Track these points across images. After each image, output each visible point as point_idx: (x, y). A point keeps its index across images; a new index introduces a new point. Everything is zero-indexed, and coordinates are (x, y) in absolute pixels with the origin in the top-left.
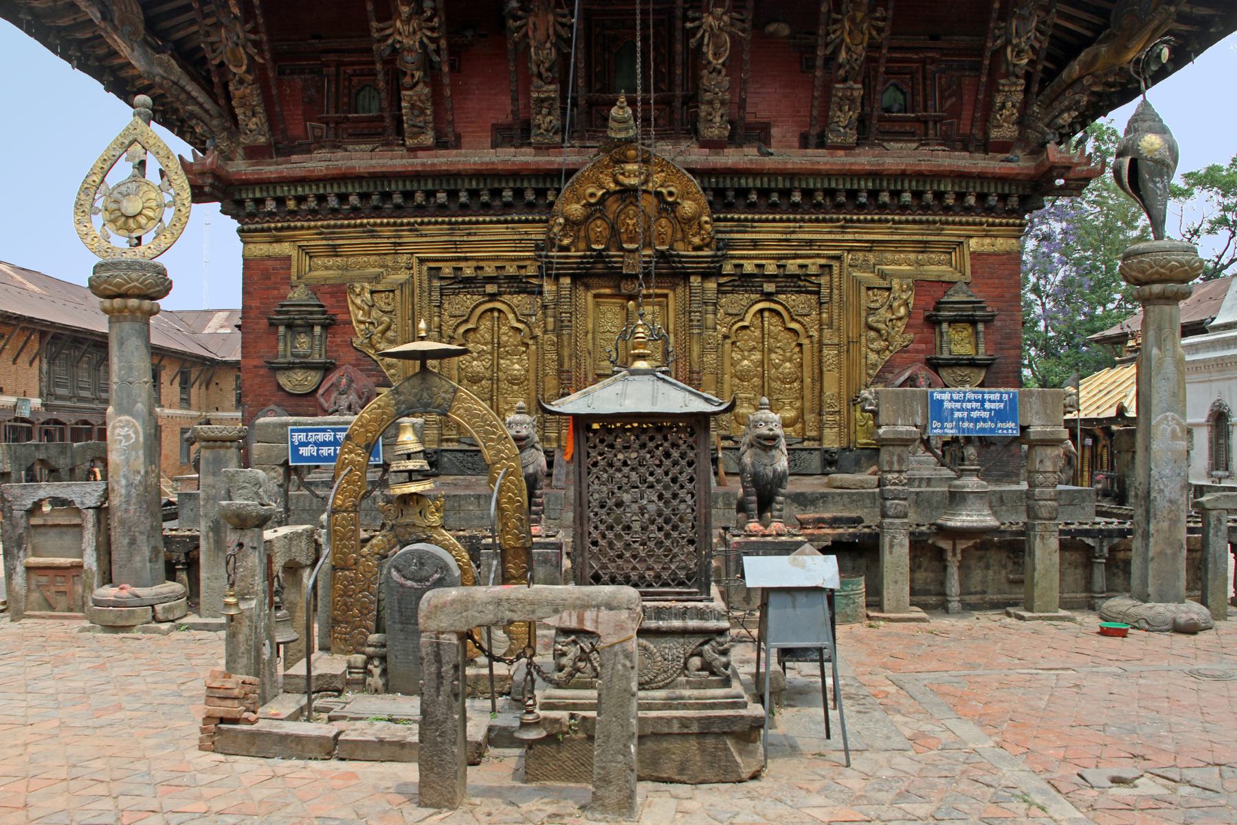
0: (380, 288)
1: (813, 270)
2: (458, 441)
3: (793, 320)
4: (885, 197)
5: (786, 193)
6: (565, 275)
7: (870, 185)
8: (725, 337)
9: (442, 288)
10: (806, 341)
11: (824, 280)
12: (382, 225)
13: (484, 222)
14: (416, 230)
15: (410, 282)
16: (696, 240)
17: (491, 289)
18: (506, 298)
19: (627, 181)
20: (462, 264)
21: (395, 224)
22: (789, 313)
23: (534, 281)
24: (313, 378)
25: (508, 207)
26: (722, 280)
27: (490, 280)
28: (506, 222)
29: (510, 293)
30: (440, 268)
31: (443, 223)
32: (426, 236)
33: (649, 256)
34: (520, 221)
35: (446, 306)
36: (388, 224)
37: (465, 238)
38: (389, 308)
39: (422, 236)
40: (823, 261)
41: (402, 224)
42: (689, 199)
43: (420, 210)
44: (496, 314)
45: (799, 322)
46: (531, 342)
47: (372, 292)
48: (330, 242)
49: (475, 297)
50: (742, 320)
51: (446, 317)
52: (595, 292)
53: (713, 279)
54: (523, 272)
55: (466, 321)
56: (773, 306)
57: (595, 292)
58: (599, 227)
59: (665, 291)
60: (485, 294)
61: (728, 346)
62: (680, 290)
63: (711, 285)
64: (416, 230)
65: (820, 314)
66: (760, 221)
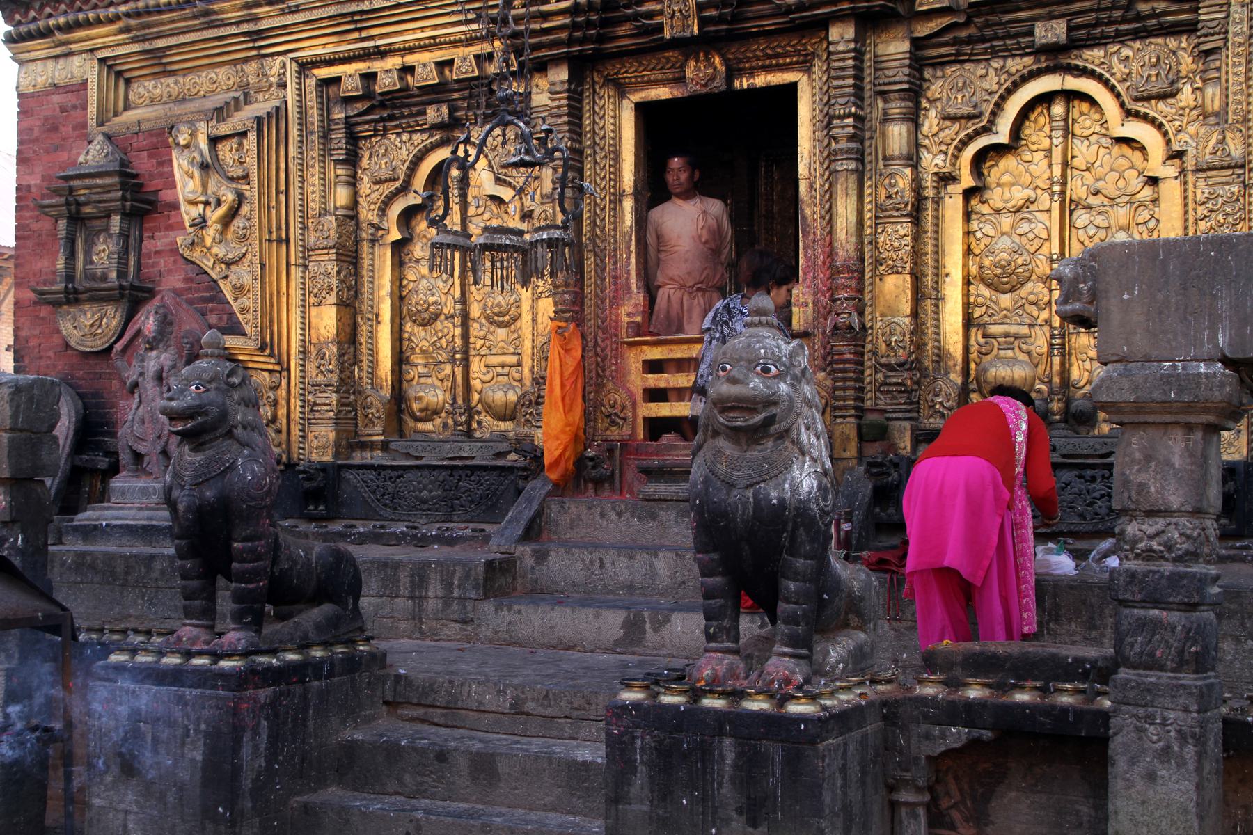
0: (224, 129)
2: (385, 446)
3: (1129, 114)
6: (556, 61)
8: (946, 179)
9: (349, 126)
15: (279, 114)
17: (433, 114)
24: (112, 317)
26: (925, 29)
30: (337, 80)
35: (365, 162)
38: (240, 172)
45: (1145, 118)
48: (147, 46)
49: (417, 138)
50: (986, 130)
51: (365, 187)
53: (901, 31)
55: (405, 188)
56: (1073, 83)
61: (953, 206)
62: (818, 68)
63: (895, 47)
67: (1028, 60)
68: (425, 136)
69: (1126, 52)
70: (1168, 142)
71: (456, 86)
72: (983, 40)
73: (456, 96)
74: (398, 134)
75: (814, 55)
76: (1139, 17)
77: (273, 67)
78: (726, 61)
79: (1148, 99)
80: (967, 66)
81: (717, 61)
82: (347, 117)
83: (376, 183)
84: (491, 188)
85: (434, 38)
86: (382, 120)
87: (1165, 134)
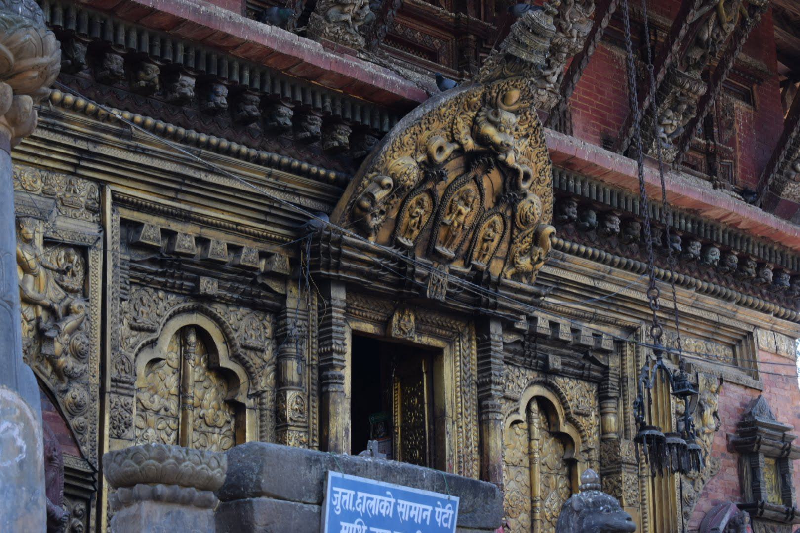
1: (607, 344)
3: (569, 419)
4: (696, 248)
5: (604, 215)
6: (340, 282)
7: (690, 225)
10: (581, 457)
11: (613, 362)
12: (73, 107)
13: (238, 155)
14: (130, 137)
16: (525, 263)
17: (207, 286)
18: (218, 309)
19: (498, 138)
20: (174, 226)
21: (95, 115)
22: (566, 408)
23: (276, 287)
25: (274, 133)
27: (213, 267)
28: (269, 163)
29: (227, 303)
30: (138, 225)
31: (175, 137)
32: (143, 152)
33: (462, 276)
34: (289, 168)
36: (84, 111)
37: (202, 176)
39: (136, 151)
40: (617, 333)
41: (108, 118)
42: (535, 191)
43: (140, 98)
44: (192, 338)
46: (250, 403)
47: (48, 242)
49: (172, 298)
52: (354, 325)
54: (262, 265)
57: (354, 325)
58: (419, 210)
59: (439, 343)
60: (194, 294)
64: (130, 137)
65: (602, 413)
66: (571, 251)
67: (535, 374)
68: (181, 298)
69: (571, 384)
70: (583, 442)
71: (229, 268)
72: (523, 355)
73: (225, 275)
74: (156, 290)
75: (460, 335)
76: (583, 367)
77: (84, 190)
78: (416, 319)
79: (578, 414)
80: (510, 366)
81: (412, 318)
82: (131, 261)
83: (132, 328)
84: (225, 362)
85: (237, 224)
86: (156, 274)
87: (582, 437)
